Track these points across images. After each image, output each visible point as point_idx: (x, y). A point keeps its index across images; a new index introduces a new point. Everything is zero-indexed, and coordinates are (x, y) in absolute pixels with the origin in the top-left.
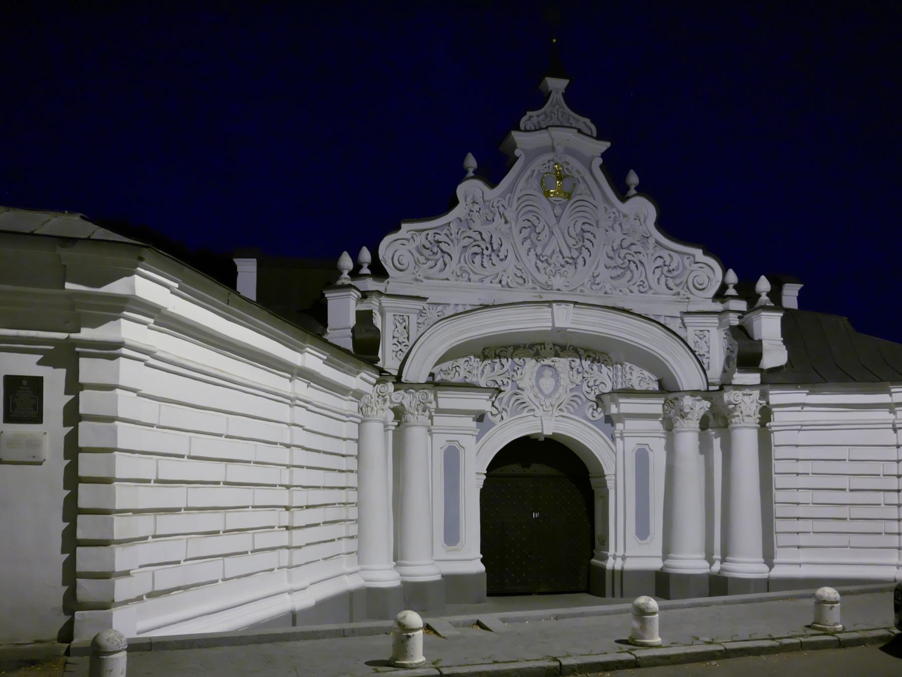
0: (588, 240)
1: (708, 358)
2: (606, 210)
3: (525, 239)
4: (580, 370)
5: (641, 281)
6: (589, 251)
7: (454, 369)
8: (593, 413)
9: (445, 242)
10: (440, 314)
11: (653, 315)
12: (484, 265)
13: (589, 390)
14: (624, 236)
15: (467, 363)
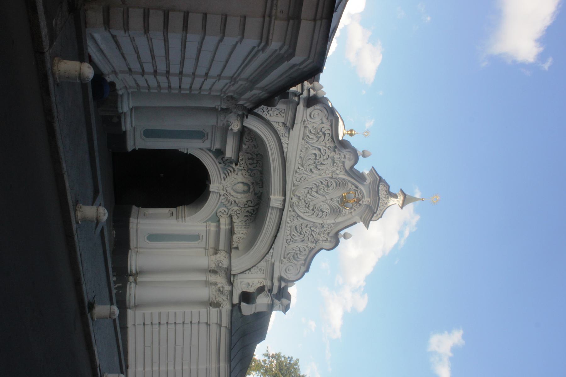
0: (318, 215)
1: (249, 273)
2: (333, 224)
3: (321, 182)
4: (246, 206)
6: (312, 215)
7: (251, 139)
8: (221, 212)
9: (324, 140)
10: (283, 135)
11: (274, 247)
12: (309, 160)
13: (235, 211)
14: (318, 233)
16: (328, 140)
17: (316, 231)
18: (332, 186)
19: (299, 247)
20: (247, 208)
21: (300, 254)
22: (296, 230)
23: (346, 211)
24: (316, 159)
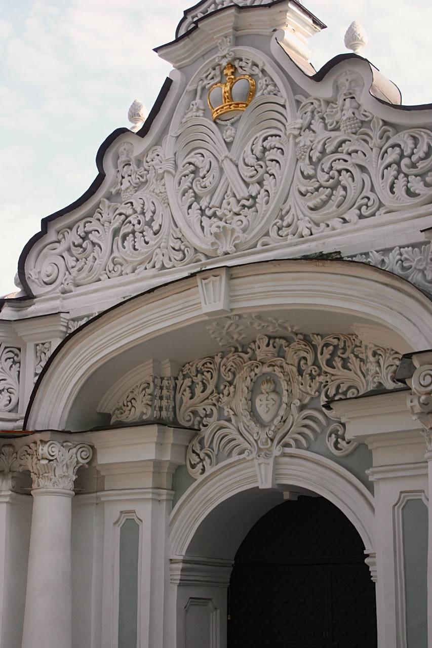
0: (272, 160)
5: (363, 198)
7: (129, 404)
8: (336, 443)
15: (144, 391)
16: (99, 220)
17: (322, 142)
18: (192, 160)
19: (382, 167)
20: (319, 367)
21: (410, 157)
22: (325, 203)
23: (259, 86)
24: (133, 232)
